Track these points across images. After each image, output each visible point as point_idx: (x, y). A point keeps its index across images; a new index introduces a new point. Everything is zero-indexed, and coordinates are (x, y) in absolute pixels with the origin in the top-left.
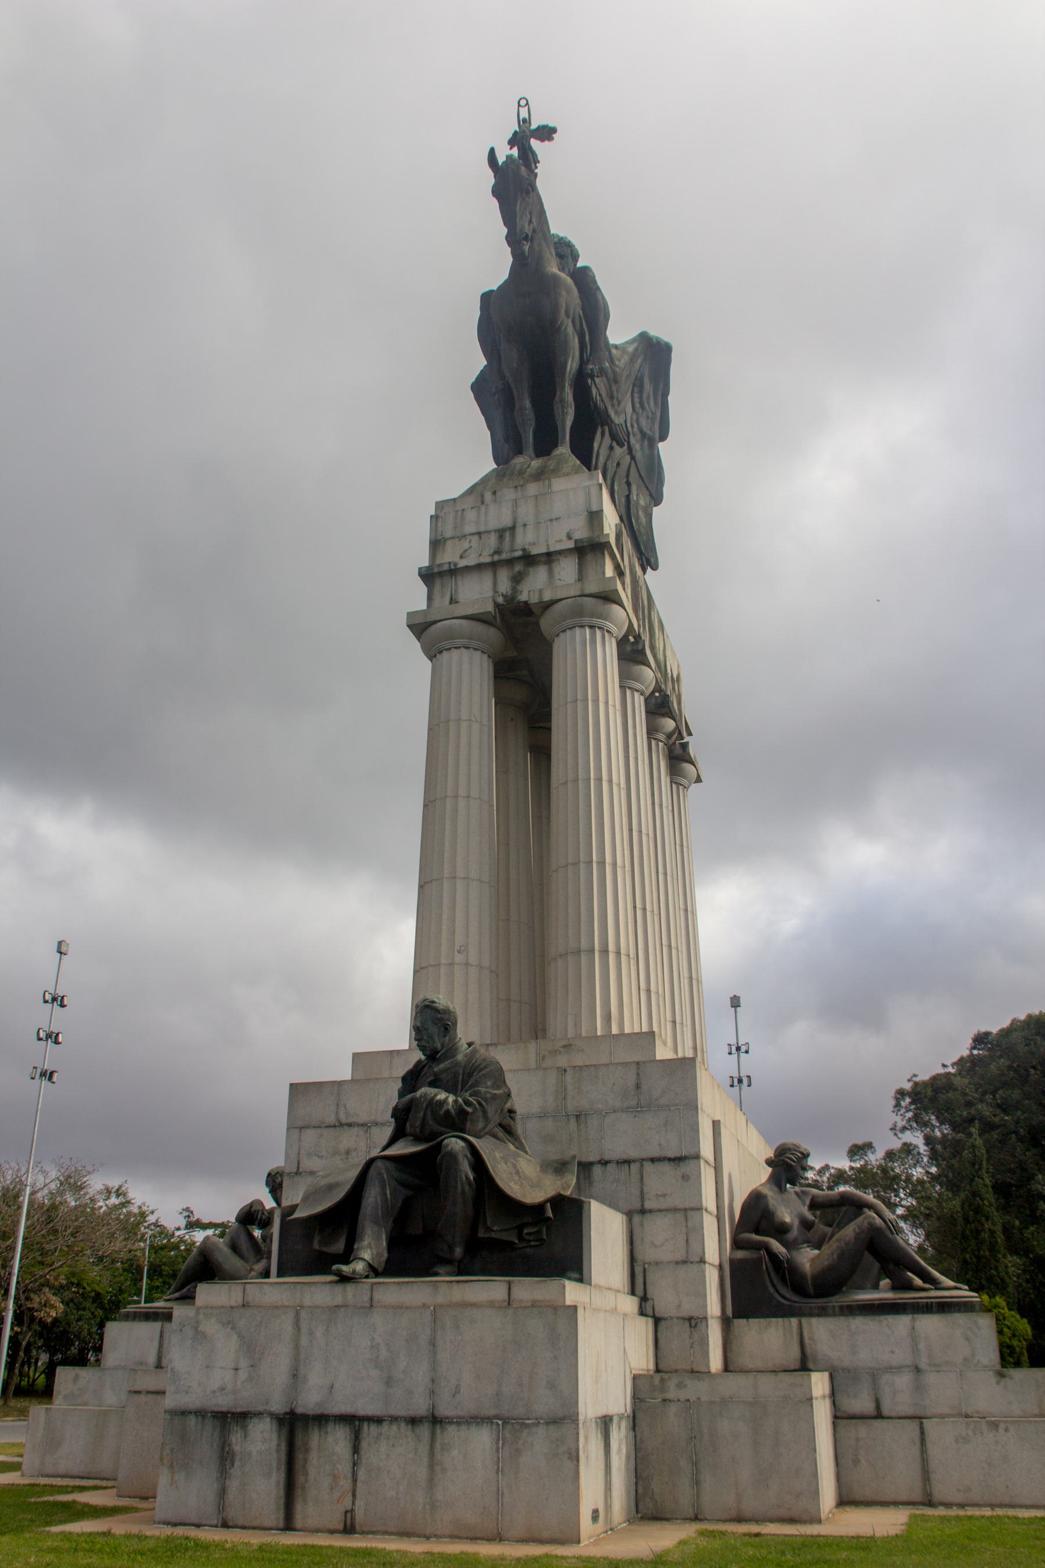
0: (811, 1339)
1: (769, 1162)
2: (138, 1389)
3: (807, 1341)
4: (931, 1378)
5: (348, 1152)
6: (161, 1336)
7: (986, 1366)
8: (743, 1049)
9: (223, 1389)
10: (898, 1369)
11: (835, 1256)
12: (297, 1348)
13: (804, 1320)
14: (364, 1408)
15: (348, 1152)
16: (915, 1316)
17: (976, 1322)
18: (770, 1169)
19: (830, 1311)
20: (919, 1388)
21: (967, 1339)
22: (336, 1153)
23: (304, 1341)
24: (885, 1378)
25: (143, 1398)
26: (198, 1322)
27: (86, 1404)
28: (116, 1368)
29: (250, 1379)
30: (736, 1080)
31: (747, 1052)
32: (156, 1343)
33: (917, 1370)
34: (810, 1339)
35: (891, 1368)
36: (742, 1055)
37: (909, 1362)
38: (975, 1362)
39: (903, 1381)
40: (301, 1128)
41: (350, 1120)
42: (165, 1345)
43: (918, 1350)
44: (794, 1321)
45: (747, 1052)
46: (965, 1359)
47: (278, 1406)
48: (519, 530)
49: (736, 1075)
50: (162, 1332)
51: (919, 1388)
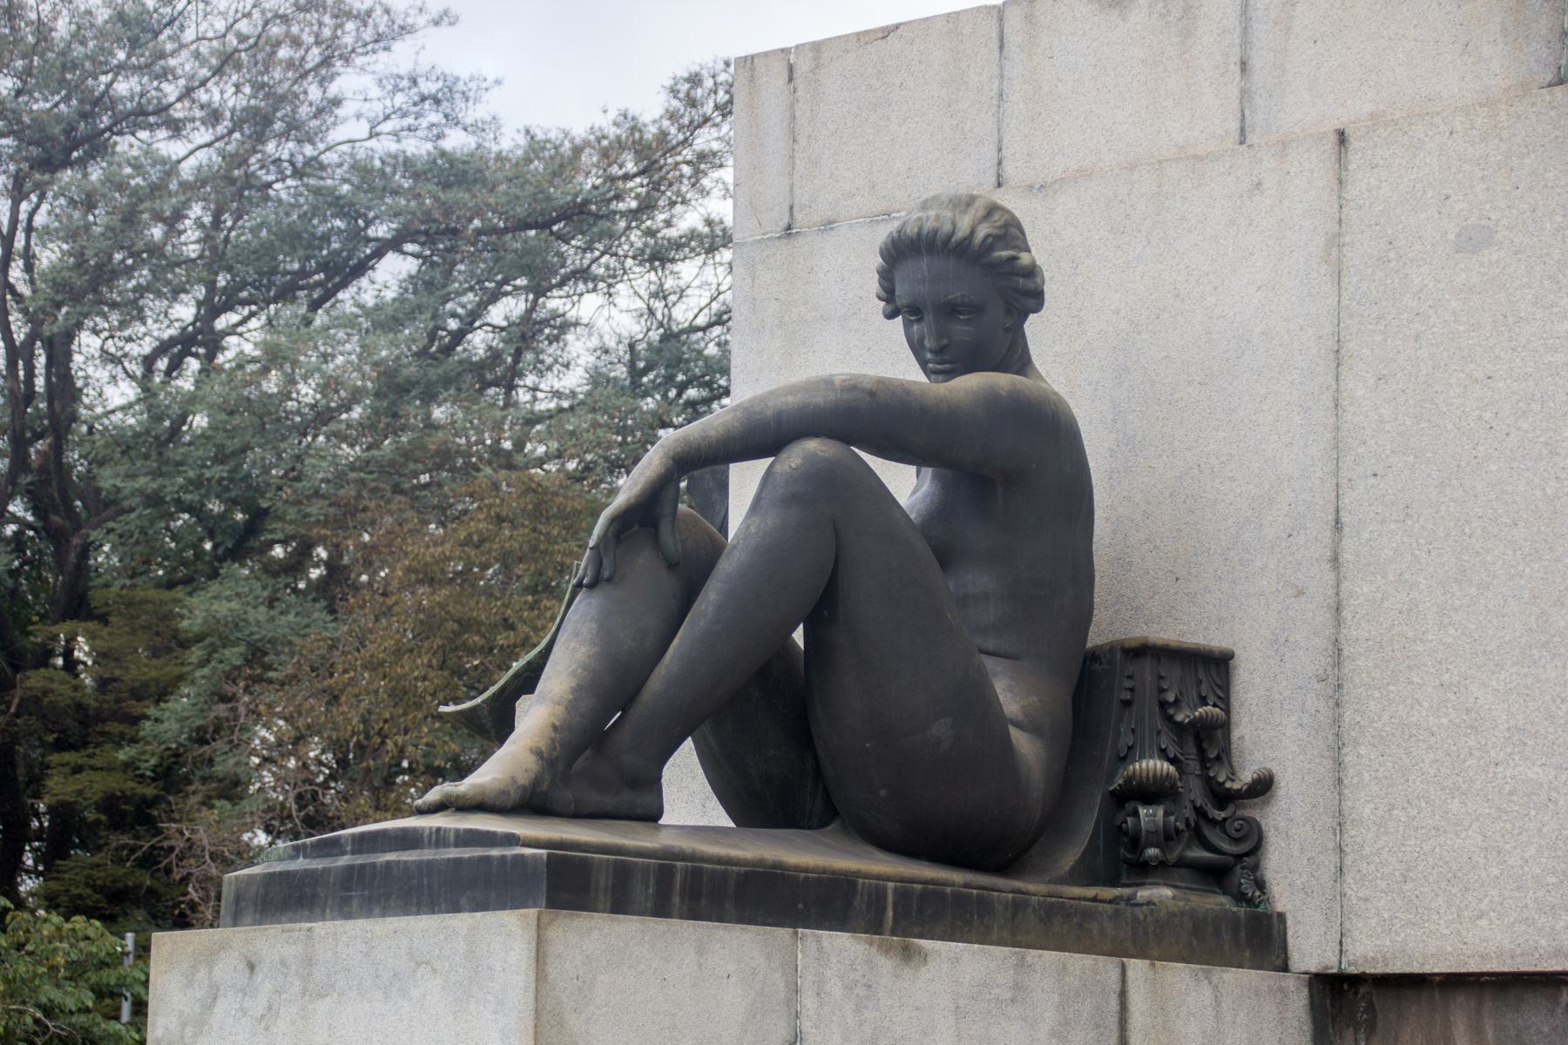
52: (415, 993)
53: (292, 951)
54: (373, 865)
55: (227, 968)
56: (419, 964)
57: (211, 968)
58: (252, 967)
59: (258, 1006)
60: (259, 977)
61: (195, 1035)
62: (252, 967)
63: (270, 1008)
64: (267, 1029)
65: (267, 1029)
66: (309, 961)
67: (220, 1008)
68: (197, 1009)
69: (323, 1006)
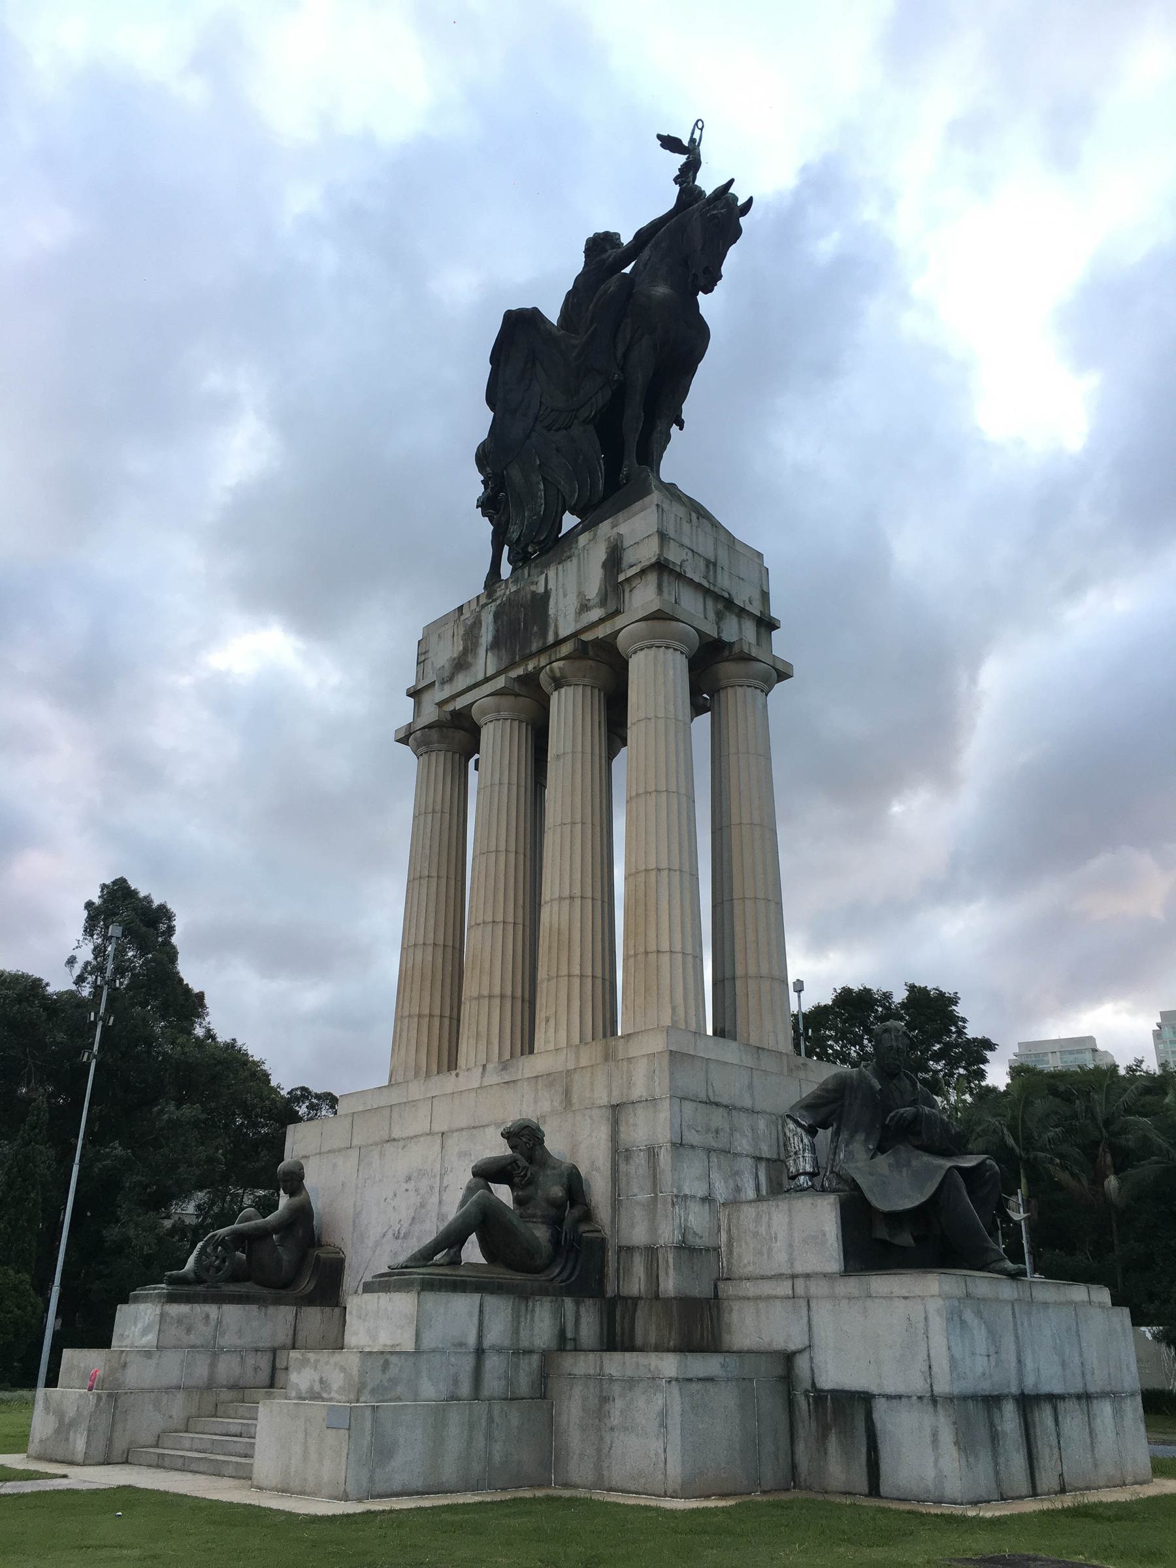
2: (690, 1376)
5: (717, 1132)
6: (481, 1312)
9: (984, 1374)
12: (1017, 1337)
14: (1058, 1389)
15: (717, 1132)
22: (708, 1130)
23: (1020, 1332)
25: (695, 1387)
26: (961, 1311)
27: (399, 1399)
28: (434, 1351)
29: (997, 1365)
32: (475, 1320)
40: (682, 1099)
41: (717, 1100)
42: (486, 1323)
47: (1014, 1390)
48: (719, 570)
50: (481, 1305)
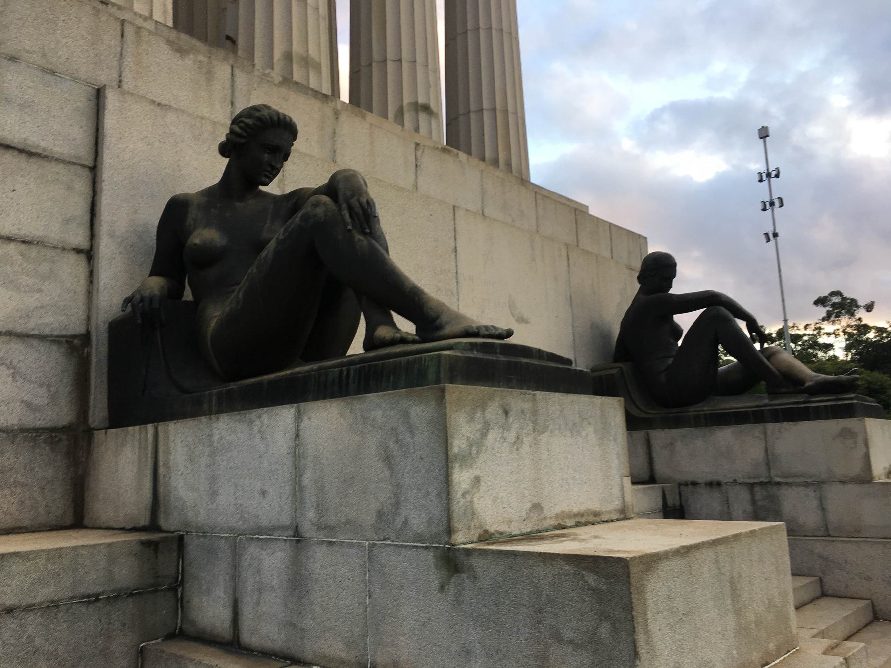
0: (166, 464)
1: (224, 150)
3: (162, 470)
4: (320, 560)
7: (419, 538)
8: (773, 174)
10: (261, 534)
11: (240, 294)
13: (162, 427)
16: (303, 405)
17: (406, 415)
18: (226, 161)
19: (206, 406)
20: (298, 583)
21: (388, 460)
24: (252, 551)
30: (768, 204)
31: (777, 176)
33: (298, 538)
34: (164, 465)
35: (260, 530)
36: (773, 180)
37: (285, 519)
38: (399, 521)
39: (271, 562)
43: (302, 489)
44: (150, 427)
45: (777, 176)
46: (380, 514)
49: (767, 199)
51: (298, 583)
52: (583, 434)
53: (526, 406)
54: (521, 363)
55: (493, 411)
56: (583, 419)
57: (484, 411)
58: (506, 413)
59: (512, 436)
60: (511, 419)
61: (477, 452)
62: (506, 413)
63: (518, 438)
64: (517, 450)
65: (517, 450)
66: (535, 412)
67: (491, 436)
68: (478, 435)
69: (544, 438)
